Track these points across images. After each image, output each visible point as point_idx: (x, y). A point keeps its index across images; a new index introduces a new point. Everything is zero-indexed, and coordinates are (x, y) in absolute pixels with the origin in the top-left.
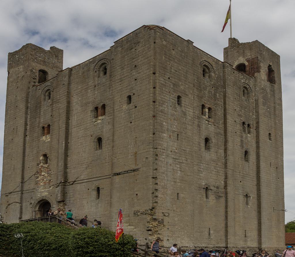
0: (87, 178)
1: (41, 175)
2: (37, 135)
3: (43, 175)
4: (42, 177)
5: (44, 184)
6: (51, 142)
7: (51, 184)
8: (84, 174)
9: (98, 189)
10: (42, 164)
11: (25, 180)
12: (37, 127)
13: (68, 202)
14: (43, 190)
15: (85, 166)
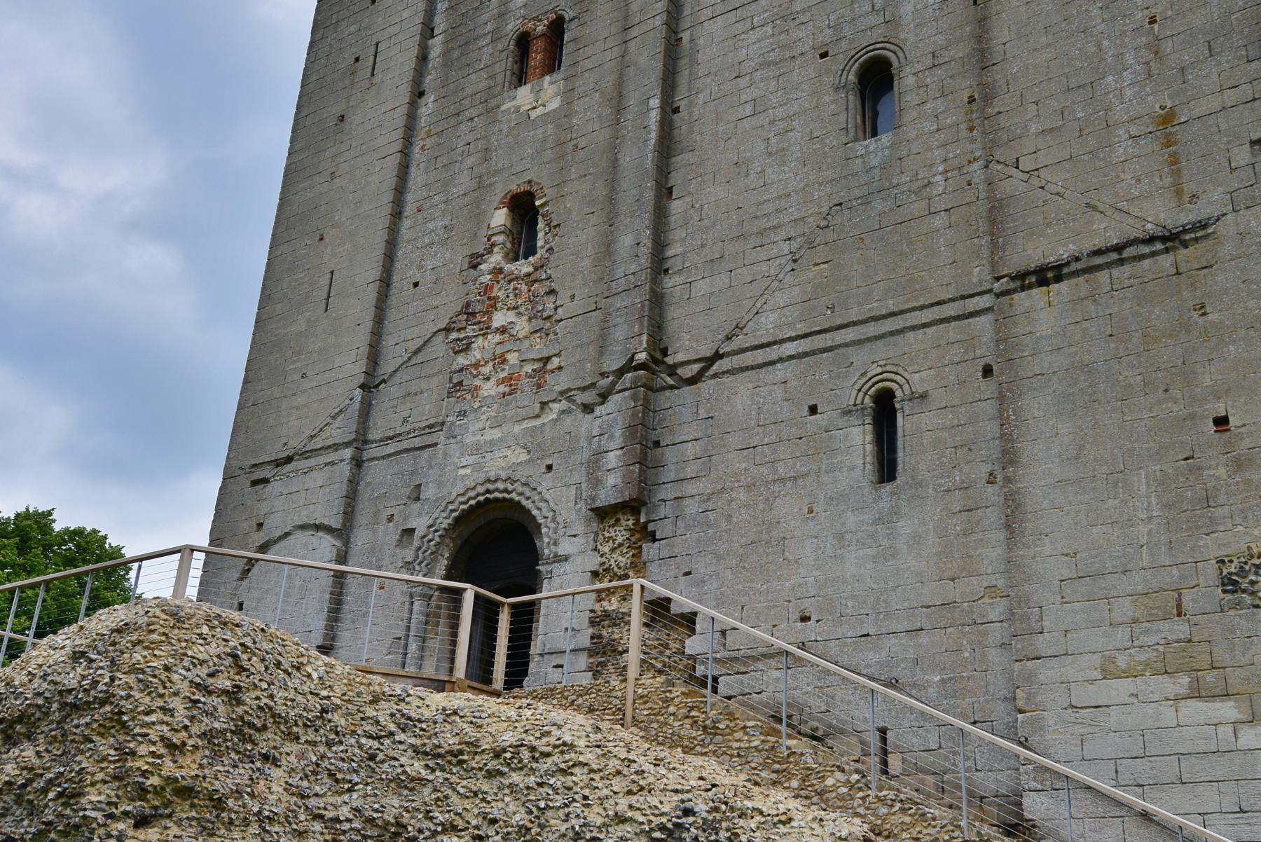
0: (801, 328)
1: (486, 330)
2: (483, 85)
3: (503, 330)
4: (498, 338)
5: (502, 388)
6: (567, 111)
7: (557, 383)
8: (780, 299)
9: (884, 411)
10: (496, 258)
11: (387, 367)
12: (488, 39)
13: (663, 511)
14: (496, 434)
15: (786, 247)
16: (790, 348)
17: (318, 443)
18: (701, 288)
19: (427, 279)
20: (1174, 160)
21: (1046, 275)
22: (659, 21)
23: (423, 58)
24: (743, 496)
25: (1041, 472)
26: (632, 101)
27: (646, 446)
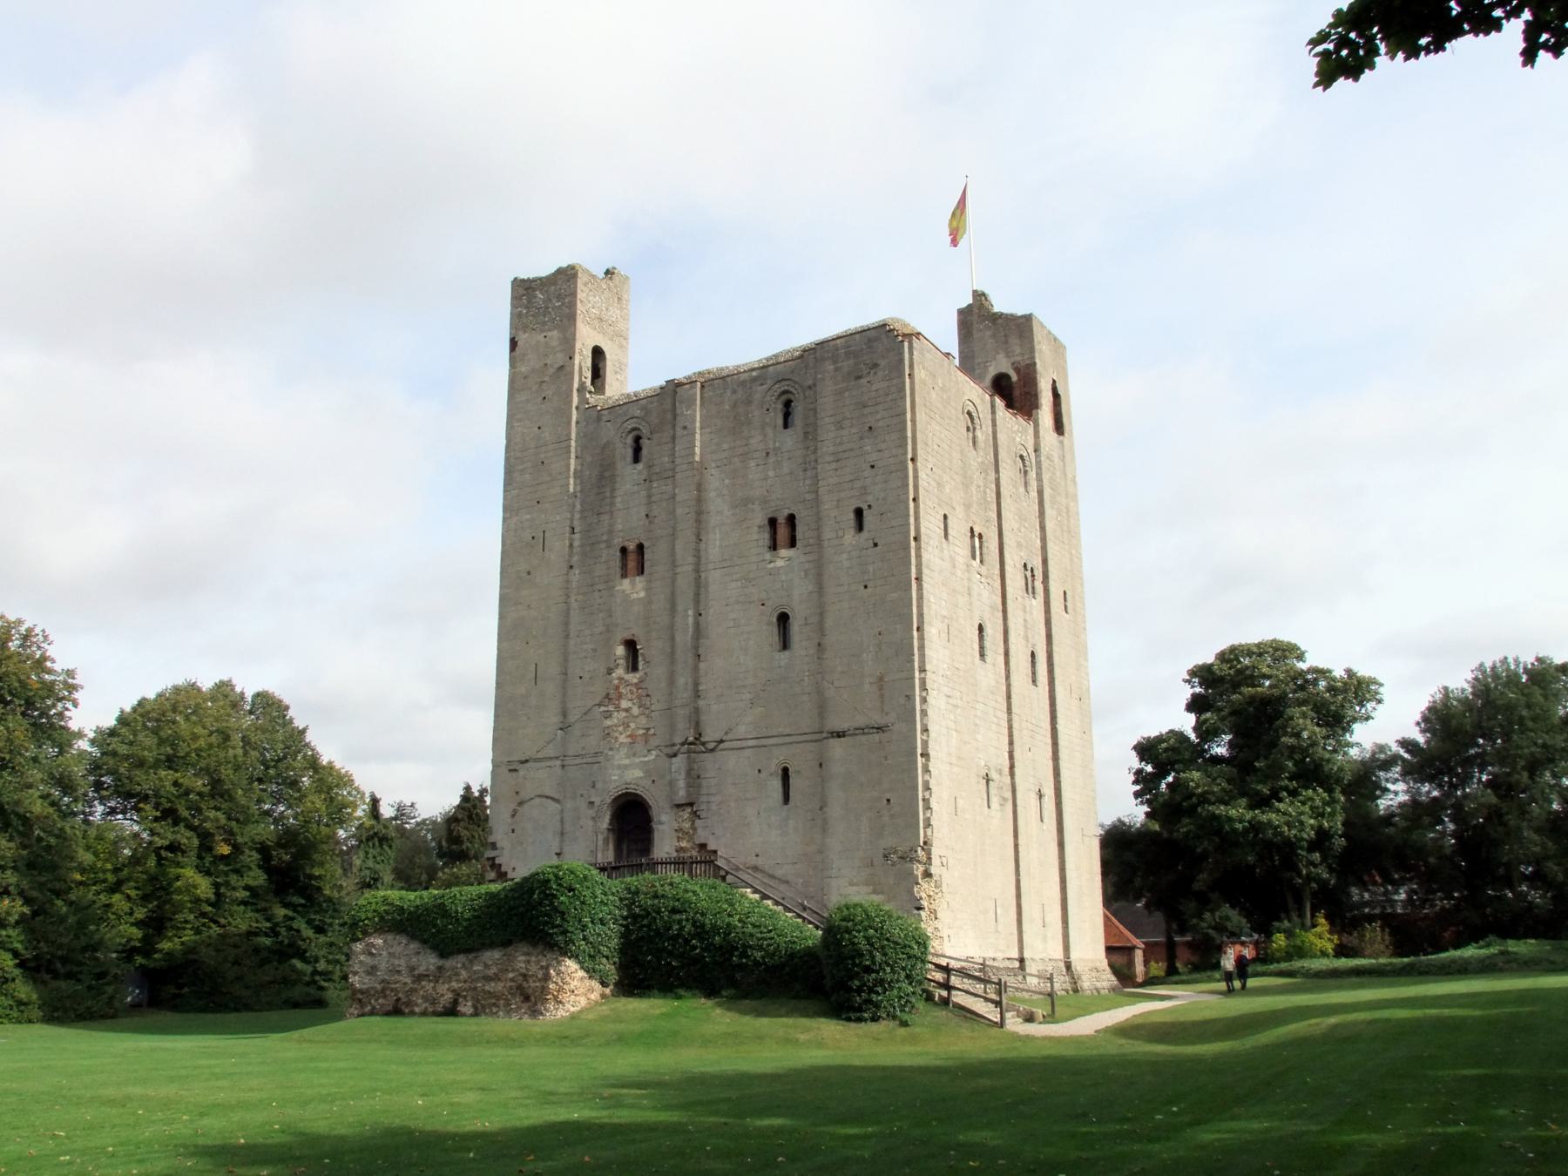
1: (618, 708)
3: (627, 710)
6: (648, 602)
7: (654, 742)
10: (620, 672)
11: (572, 719)
13: (703, 807)
16: (751, 743)
17: (540, 755)
18: (714, 708)
19: (587, 676)
20: (882, 696)
21: (840, 735)
22: (690, 568)
23: (571, 545)
24: (733, 804)
25: (835, 811)
26: (680, 608)
27: (694, 778)
